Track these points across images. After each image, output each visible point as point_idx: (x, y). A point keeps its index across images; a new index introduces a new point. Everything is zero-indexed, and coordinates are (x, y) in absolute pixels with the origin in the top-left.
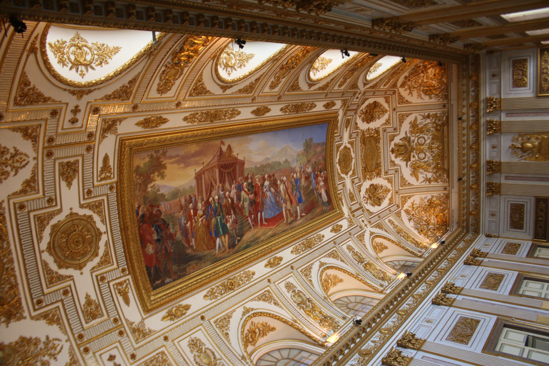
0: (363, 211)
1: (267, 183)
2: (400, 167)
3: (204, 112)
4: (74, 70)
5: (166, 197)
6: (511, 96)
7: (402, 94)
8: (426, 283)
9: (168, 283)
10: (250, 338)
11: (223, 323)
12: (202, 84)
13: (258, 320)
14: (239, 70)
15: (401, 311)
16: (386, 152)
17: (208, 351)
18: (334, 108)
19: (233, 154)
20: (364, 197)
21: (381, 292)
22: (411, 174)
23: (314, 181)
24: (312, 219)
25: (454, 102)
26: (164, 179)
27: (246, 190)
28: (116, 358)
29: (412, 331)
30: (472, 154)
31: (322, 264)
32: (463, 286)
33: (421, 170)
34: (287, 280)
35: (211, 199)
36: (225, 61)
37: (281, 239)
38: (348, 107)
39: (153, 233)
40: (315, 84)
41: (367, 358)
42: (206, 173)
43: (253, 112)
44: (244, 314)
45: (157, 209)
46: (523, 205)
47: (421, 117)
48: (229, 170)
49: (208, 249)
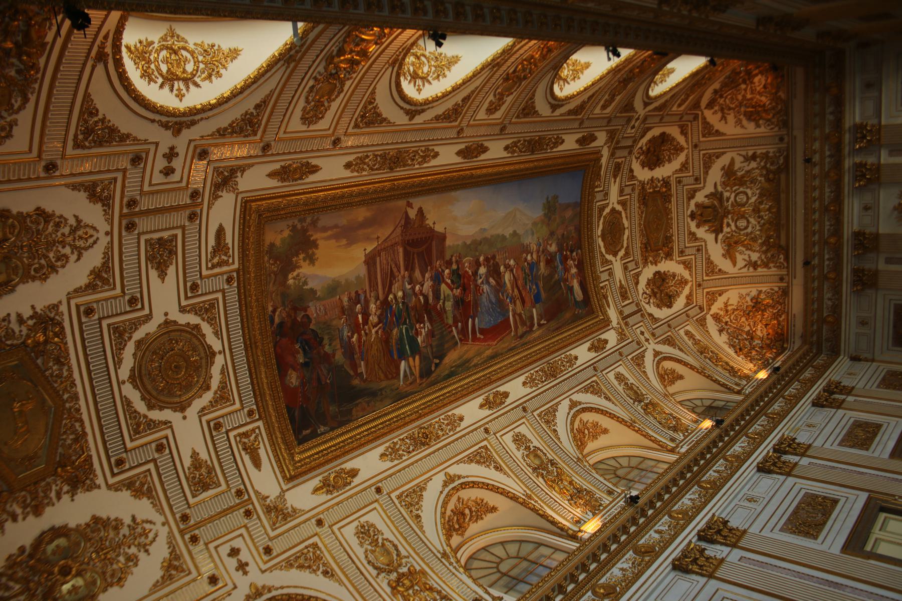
0: (642, 315)
1: (482, 270)
2: (705, 241)
3: (379, 153)
4: (167, 88)
5: (319, 293)
7: (708, 120)
8: (748, 437)
9: (322, 434)
10: (455, 522)
11: (412, 499)
12: (375, 108)
13: (469, 494)
14: (435, 83)
15: (705, 482)
16: (681, 217)
17: (387, 543)
18: (593, 144)
19: (427, 222)
20: (645, 293)
21: (672, 451)
23: (560, 267)
24: (557, 329)
25: (798, 134)
26: (314, 265)
27: (449, 281)
28: (241, 553)
29: (723, 516)
30: (829, 220)
31: (573, 404)
32: (810, 442)
33: (741, 248)
34: (516, 430)
35: (391, 296)
36: (411, 69)
37: (506, 363)
38: (618, 143)
39: (298, 353)
40: (562, 105)
41: (647, 559)
42: (383, 254)
43: (459, 153)
44: (445, 485)
45: (303, 314)
47: (742, 159)
48: (420, 250)
49: (387, 378)
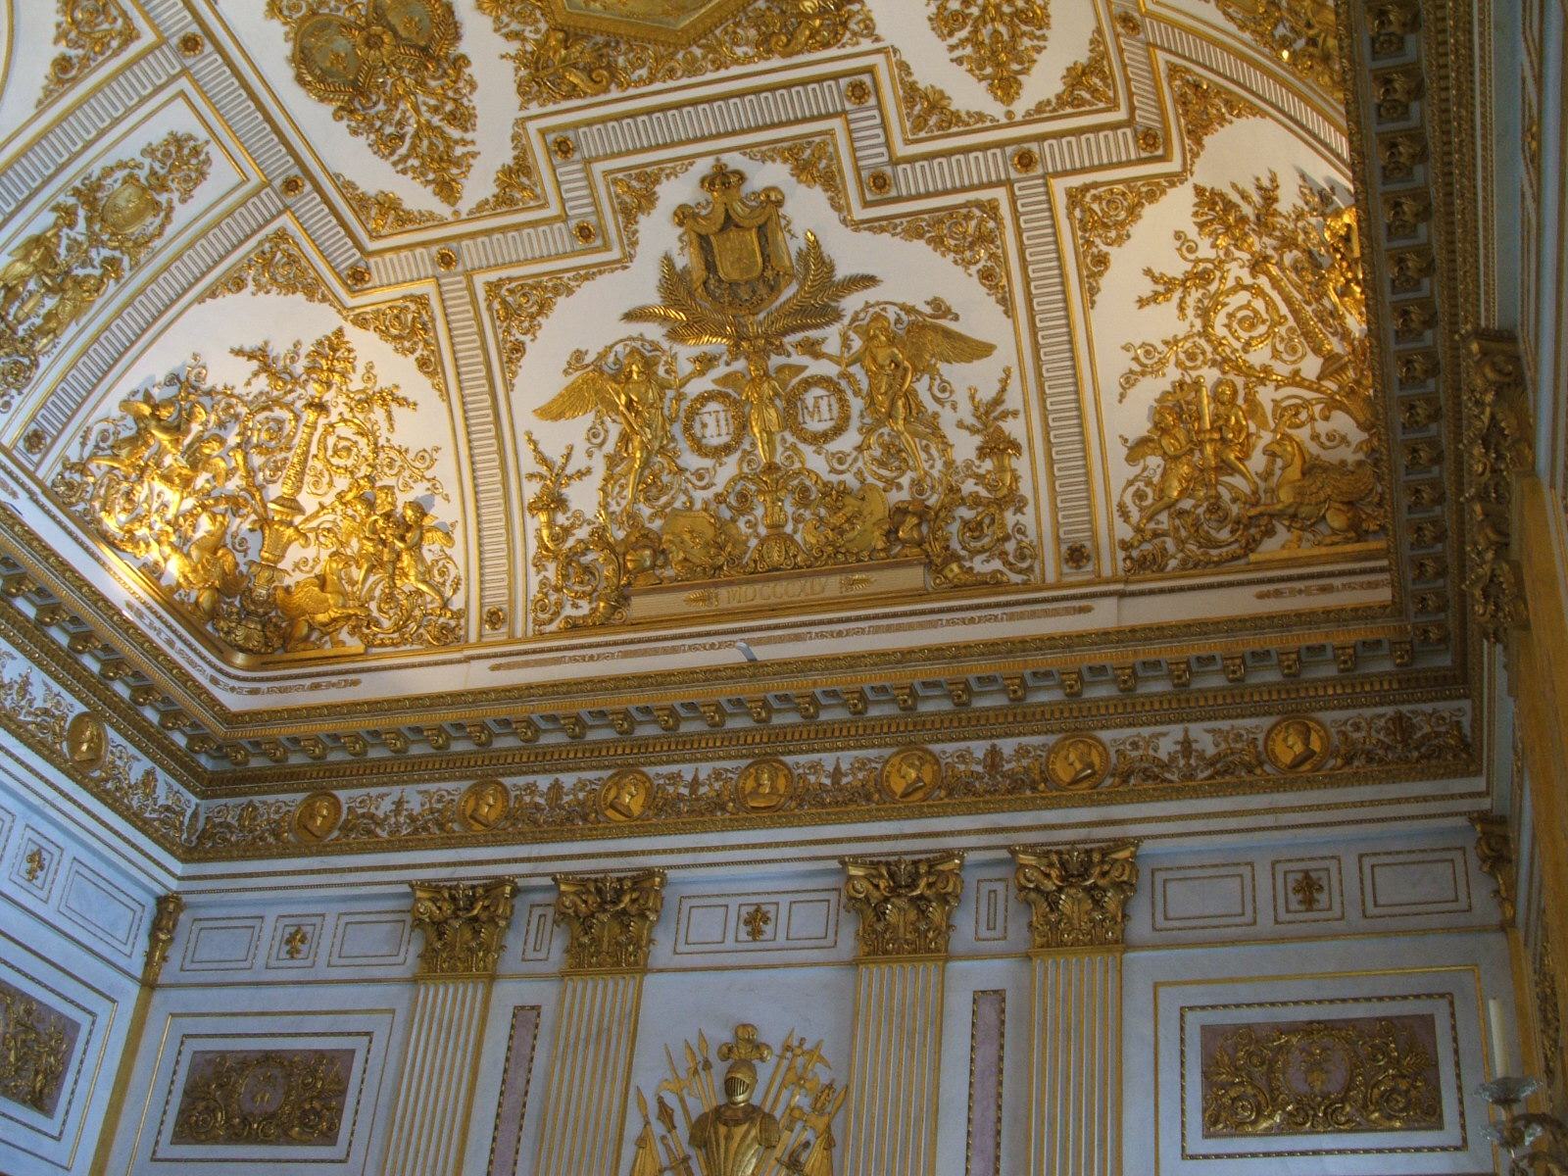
2: (623, 263)
6: (1138, 1026)
7: (1148, 211)
16: (704, 120)
22: (579, 355)
30: (717, 775)
33: (614, 431)
46: (329, 1137)
47: (987, 394)
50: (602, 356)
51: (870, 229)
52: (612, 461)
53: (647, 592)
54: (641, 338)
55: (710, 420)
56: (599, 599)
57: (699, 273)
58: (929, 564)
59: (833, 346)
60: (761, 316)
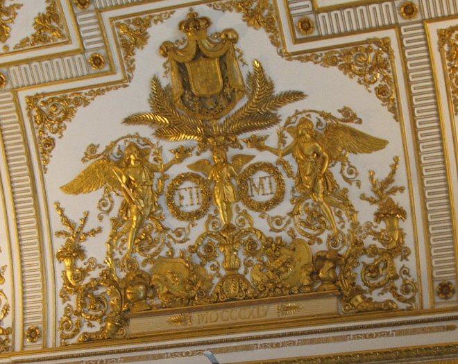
2: (124, 82)
22: (93, 148)
33: (118, 202)
47: (381, 175)
50: (109, 149)
51: (299, 59)
52: (116, 223)
53: (141, 316)
54: (137, 136)
55: (185, 194)
56: (107, 320)
57: (178, 90)
58: (341, 296)
59: (272, 142)
60: (222, 120)
